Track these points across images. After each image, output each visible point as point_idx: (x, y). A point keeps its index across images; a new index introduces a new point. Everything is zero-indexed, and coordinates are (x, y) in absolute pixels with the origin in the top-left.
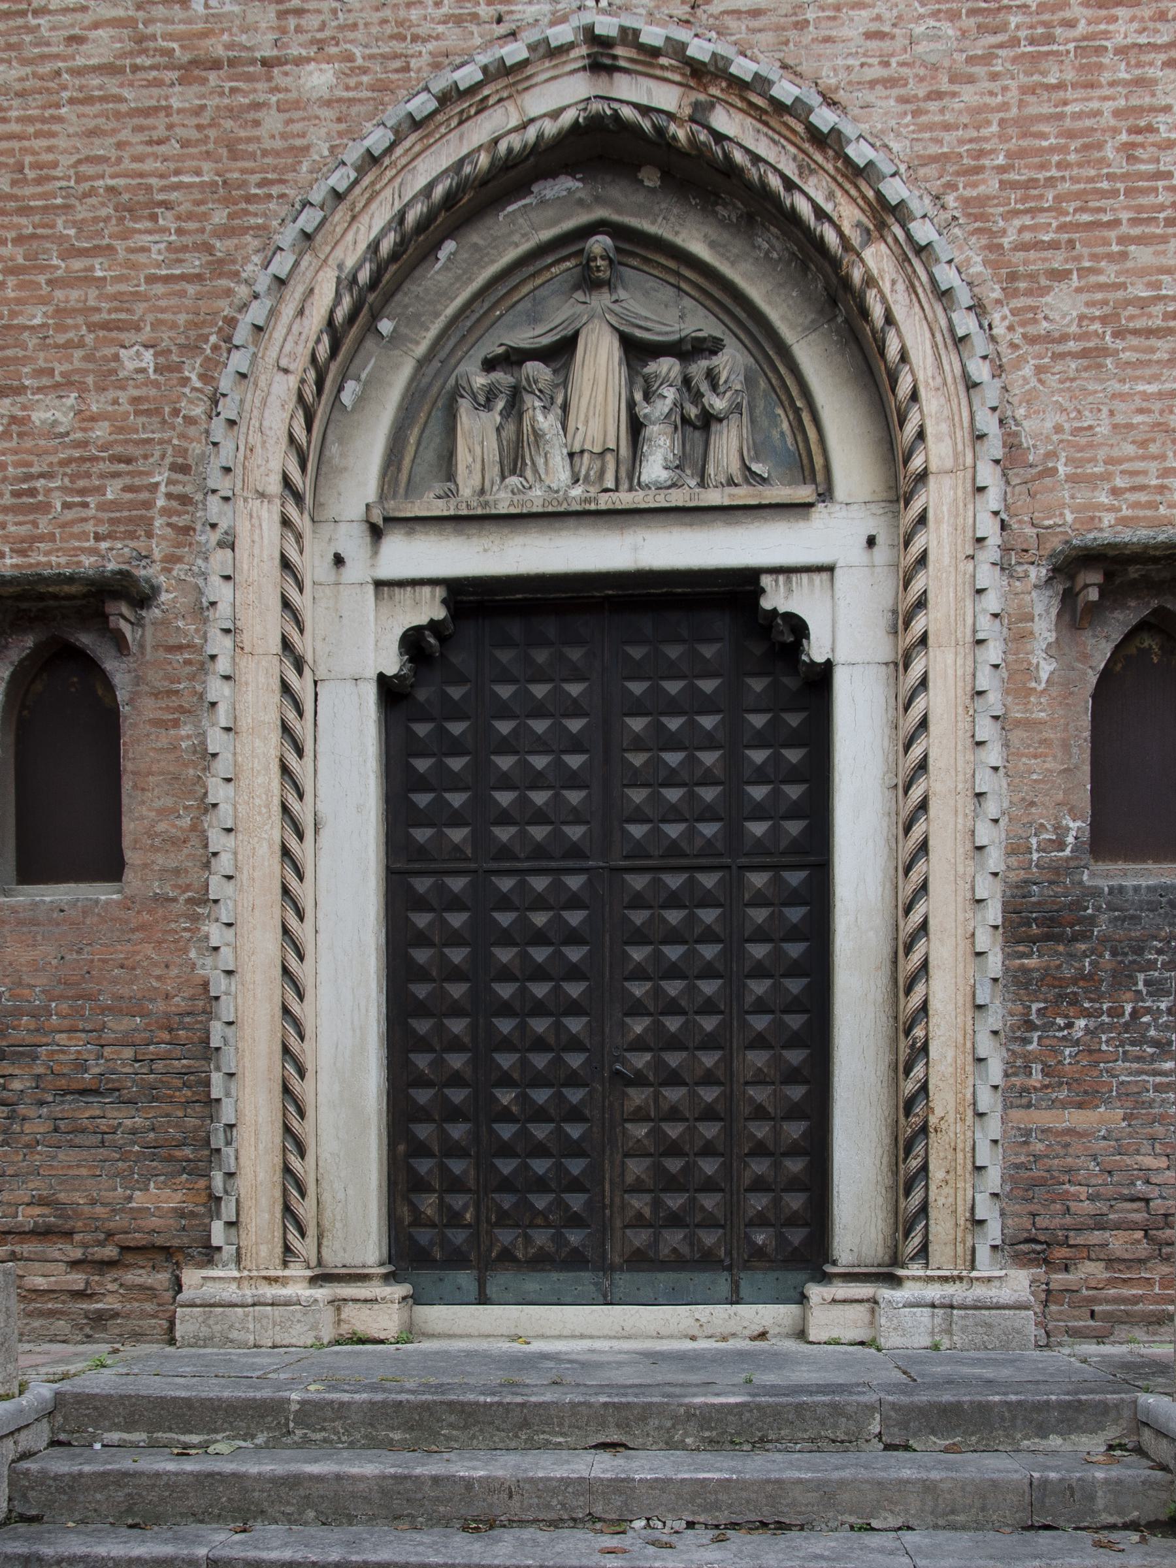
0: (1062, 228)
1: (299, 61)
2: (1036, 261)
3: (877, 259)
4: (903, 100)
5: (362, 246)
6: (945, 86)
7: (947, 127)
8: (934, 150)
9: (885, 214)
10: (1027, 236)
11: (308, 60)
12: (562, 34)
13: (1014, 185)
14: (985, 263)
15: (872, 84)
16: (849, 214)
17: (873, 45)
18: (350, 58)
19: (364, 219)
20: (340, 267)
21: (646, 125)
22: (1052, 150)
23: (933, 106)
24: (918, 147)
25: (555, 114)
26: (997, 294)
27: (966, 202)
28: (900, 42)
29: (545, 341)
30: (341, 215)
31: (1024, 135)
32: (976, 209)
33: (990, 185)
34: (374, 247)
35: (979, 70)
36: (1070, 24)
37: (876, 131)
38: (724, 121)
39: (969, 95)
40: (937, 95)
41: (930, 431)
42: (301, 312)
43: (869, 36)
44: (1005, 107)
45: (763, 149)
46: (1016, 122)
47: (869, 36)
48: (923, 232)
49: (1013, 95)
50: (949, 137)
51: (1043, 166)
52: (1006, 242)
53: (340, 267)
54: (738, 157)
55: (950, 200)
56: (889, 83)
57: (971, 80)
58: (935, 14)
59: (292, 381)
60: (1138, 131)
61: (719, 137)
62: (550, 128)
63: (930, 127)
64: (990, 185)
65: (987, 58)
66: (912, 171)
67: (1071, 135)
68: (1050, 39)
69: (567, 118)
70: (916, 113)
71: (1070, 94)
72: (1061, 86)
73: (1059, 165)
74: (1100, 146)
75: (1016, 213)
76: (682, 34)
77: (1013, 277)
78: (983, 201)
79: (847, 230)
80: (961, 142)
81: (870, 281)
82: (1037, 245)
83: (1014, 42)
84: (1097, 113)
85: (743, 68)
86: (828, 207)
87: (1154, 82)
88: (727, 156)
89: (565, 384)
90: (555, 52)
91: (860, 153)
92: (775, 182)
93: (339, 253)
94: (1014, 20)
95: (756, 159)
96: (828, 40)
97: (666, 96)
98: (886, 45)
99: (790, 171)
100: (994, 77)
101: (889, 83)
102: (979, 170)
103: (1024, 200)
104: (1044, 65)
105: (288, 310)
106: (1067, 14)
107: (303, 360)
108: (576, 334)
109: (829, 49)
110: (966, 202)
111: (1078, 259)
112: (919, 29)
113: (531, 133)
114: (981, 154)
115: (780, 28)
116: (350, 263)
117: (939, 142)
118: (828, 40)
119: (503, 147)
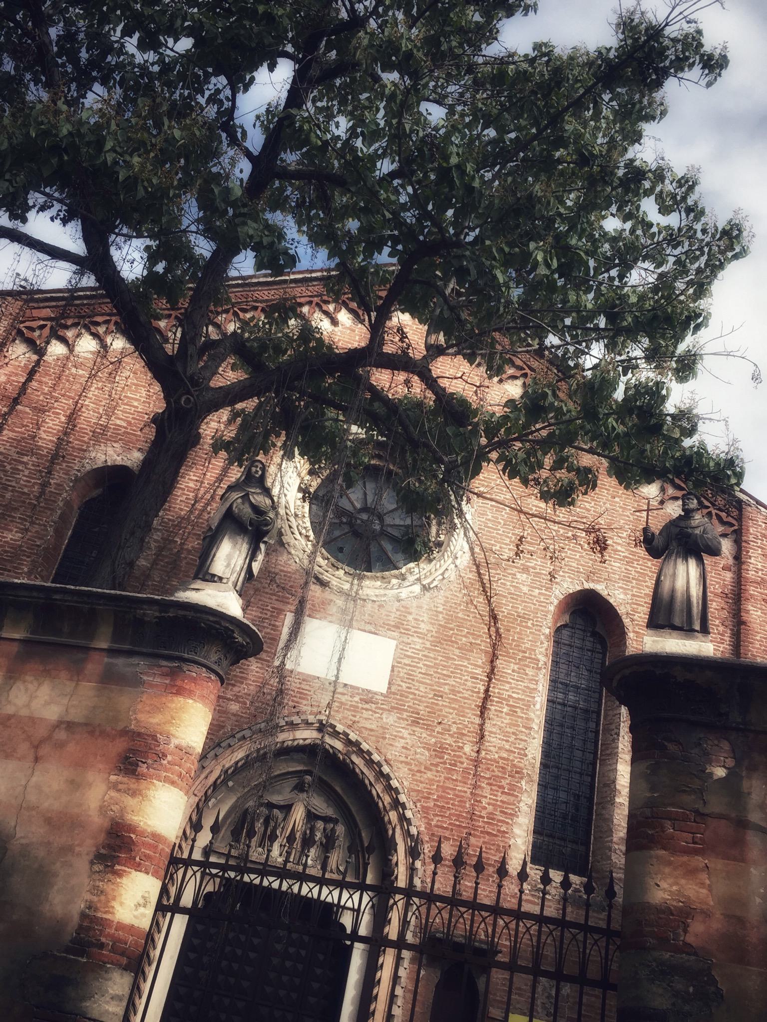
0: (450, 824)
1: (229, 699)
2: (440, 832)
3: (393, 816)
4: (409, 769)
5: (233, 762)
6: (423, 770)
7: (421, 782)
8: (416, 788)
9: (397, 804)
10: (439, 823)
11: (232, 700)
12: (311, 719)
13: (438, 806)
14: (426, 828)
15: (402, 762)
16: (387, 799)
17: (404, 750)
18: (246, 704)
19: (236, 754)
20: (224, 766)
21: (331, 751)
22: (450, 799)
23: (418, 774)
24: (412, 786)
25: (305, 740)
26: (427, 839)
27: (423, 807)
28: (412, 752)
29: (282, 803)
30: (229, 751)
31: (444, 792)
32: (425, 810)
33: (431, 804)
34: (237, 763)
35: (434, 768)
36: (462, 763)
37: (401, 778)
38: (354, 758)
39: (429, 775)
40: (419, 771)
41: (399, 877)
42: (206, 778)
43: (403, 747)
44: (439, 781)
45: (365, 770)
46: (442, 787)
47: (403, 747)
48: (409, 814)
49: (442, 779)
50: (421, 785)
51: (448, 803)
52: (433, 823)
53: (224, 766)
54: (357, 770)
55: (418, 805)
56: (407, 763)
57: (431, 770)
58: (424, 748)
59: (197, 799)
60: (477, 801)
61: (353, 763)
62: (301, 742)
63: (417, 781)
64: (431, 804)
65: (436, 765)
66: (410, 790)
67: (457, 796)
68: (455, 765)
69: (308, 742)
70: (413, 775)
71: (458, 784)
72: (456, 780)
73: (452, 804)
74: (465, 802)
75: (437, 815)
76: (348, 731)
77: (433, 835)
78: (428, 808)
79: (386, 804)
80: (425, 788)
81: (390, 822)
82: (442, 827)
83: (445, 763)
84: (466, 792)
85: (365, 746)
86: (381, 795)
87: (484, 788)
88: (354, 768)
89: (284, 819)
90: (308, 724)
91: (394, 783)
92: (367, 782)
93: (224, 762)
94: (446, 757)
95: (362, 773)
96: (391, 745)
97: (338, 745)
98: (408, 752)
99: (372, 780)
100: (437, 771)
101: (407, 763)
102: (429, 798)
103: (441, 811)
104: (453, 772)
105: (203, 776)
106: (462, 760)
107: (202, 794)
108: (292, 804)
109: (391, 748)
110: (423, 807)
111: (453, 835)
112: (418, 751)
113: (296, 743)
114: (430, 793)
115: (377, 737)
116: (227, 766)
117: (418, 786)
118: (391, 745)
119: (285, 744)
